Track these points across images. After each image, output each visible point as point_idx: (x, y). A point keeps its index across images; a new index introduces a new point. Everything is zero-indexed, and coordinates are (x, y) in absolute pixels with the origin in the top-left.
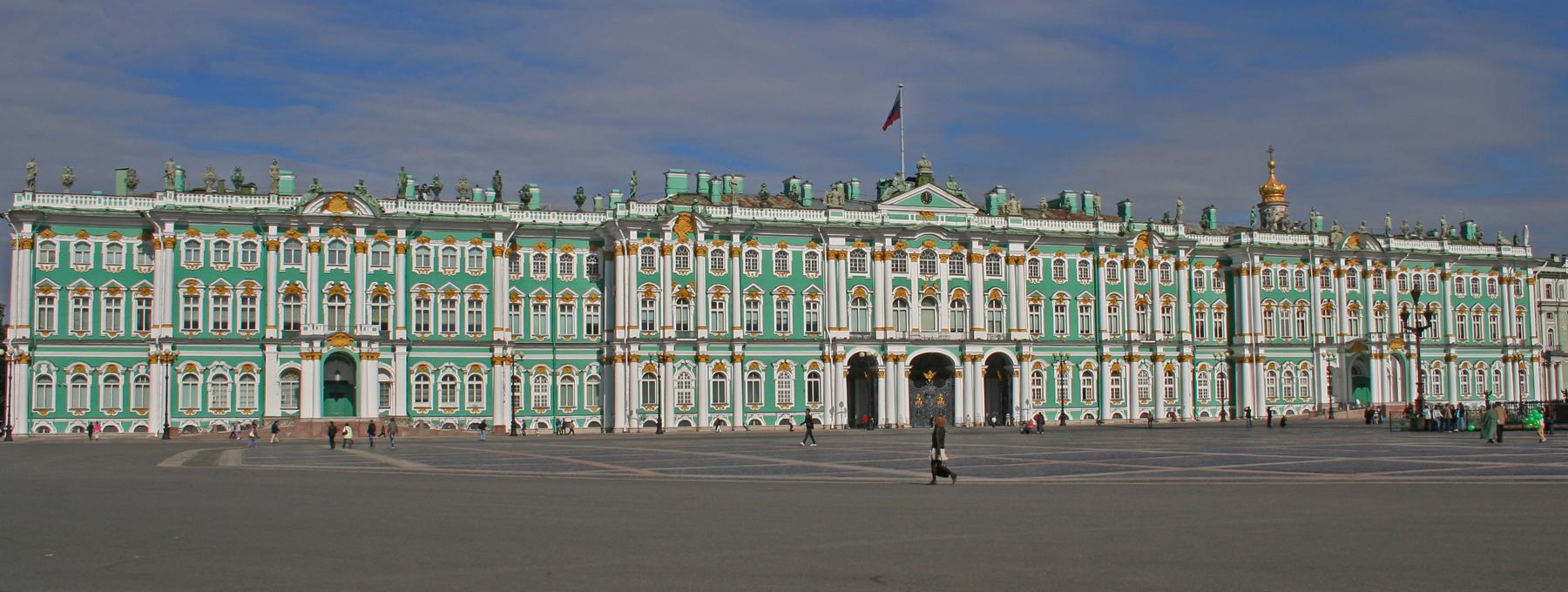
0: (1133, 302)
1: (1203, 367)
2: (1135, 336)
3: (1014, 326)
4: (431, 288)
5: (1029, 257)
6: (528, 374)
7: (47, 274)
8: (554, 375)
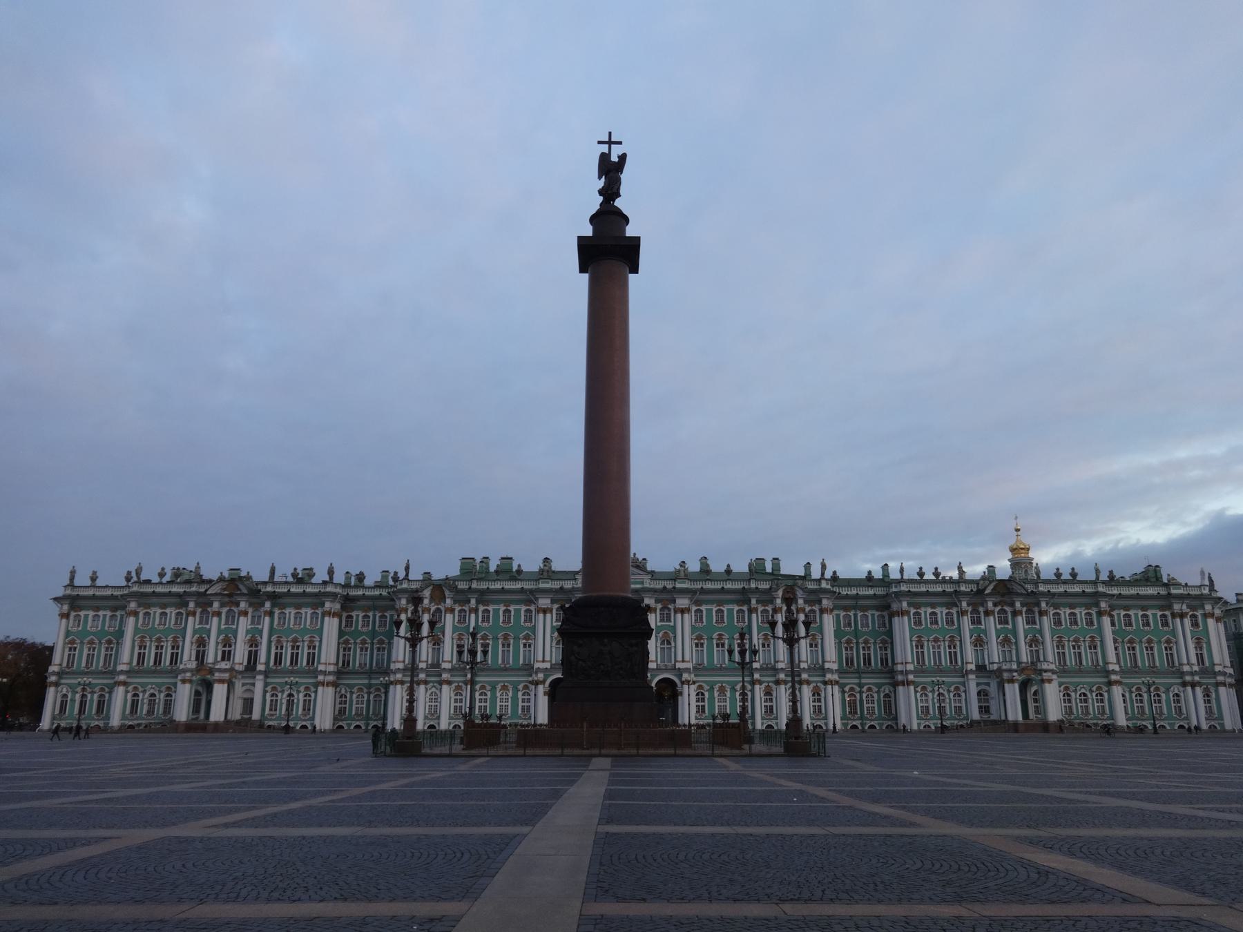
1: (869, 689)
3: (680, 658)
4: (284, 639)
6: (352, 693)
7: (73, 633)
8: (369, 693)
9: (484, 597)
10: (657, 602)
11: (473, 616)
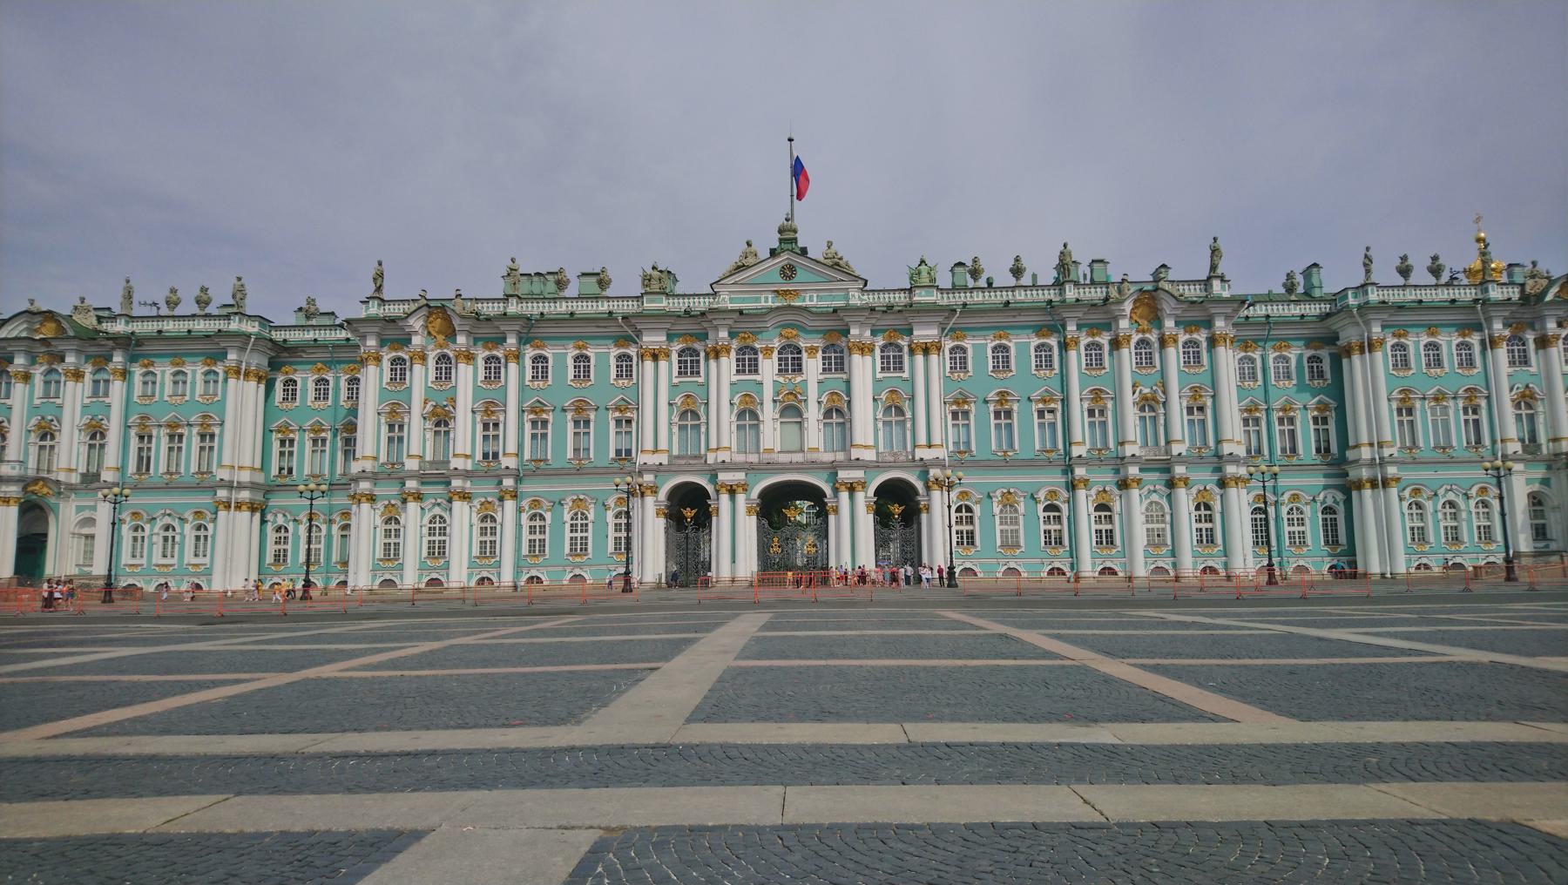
0: (1129, 398)
1: (1295, 498)
2: (1129, 450)
3: (922, 440)
5: (948, 344)
9: (531, 330)
10: (874, 333)
11: (513, 366)
